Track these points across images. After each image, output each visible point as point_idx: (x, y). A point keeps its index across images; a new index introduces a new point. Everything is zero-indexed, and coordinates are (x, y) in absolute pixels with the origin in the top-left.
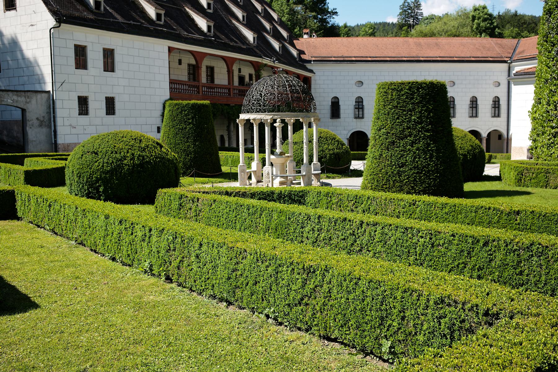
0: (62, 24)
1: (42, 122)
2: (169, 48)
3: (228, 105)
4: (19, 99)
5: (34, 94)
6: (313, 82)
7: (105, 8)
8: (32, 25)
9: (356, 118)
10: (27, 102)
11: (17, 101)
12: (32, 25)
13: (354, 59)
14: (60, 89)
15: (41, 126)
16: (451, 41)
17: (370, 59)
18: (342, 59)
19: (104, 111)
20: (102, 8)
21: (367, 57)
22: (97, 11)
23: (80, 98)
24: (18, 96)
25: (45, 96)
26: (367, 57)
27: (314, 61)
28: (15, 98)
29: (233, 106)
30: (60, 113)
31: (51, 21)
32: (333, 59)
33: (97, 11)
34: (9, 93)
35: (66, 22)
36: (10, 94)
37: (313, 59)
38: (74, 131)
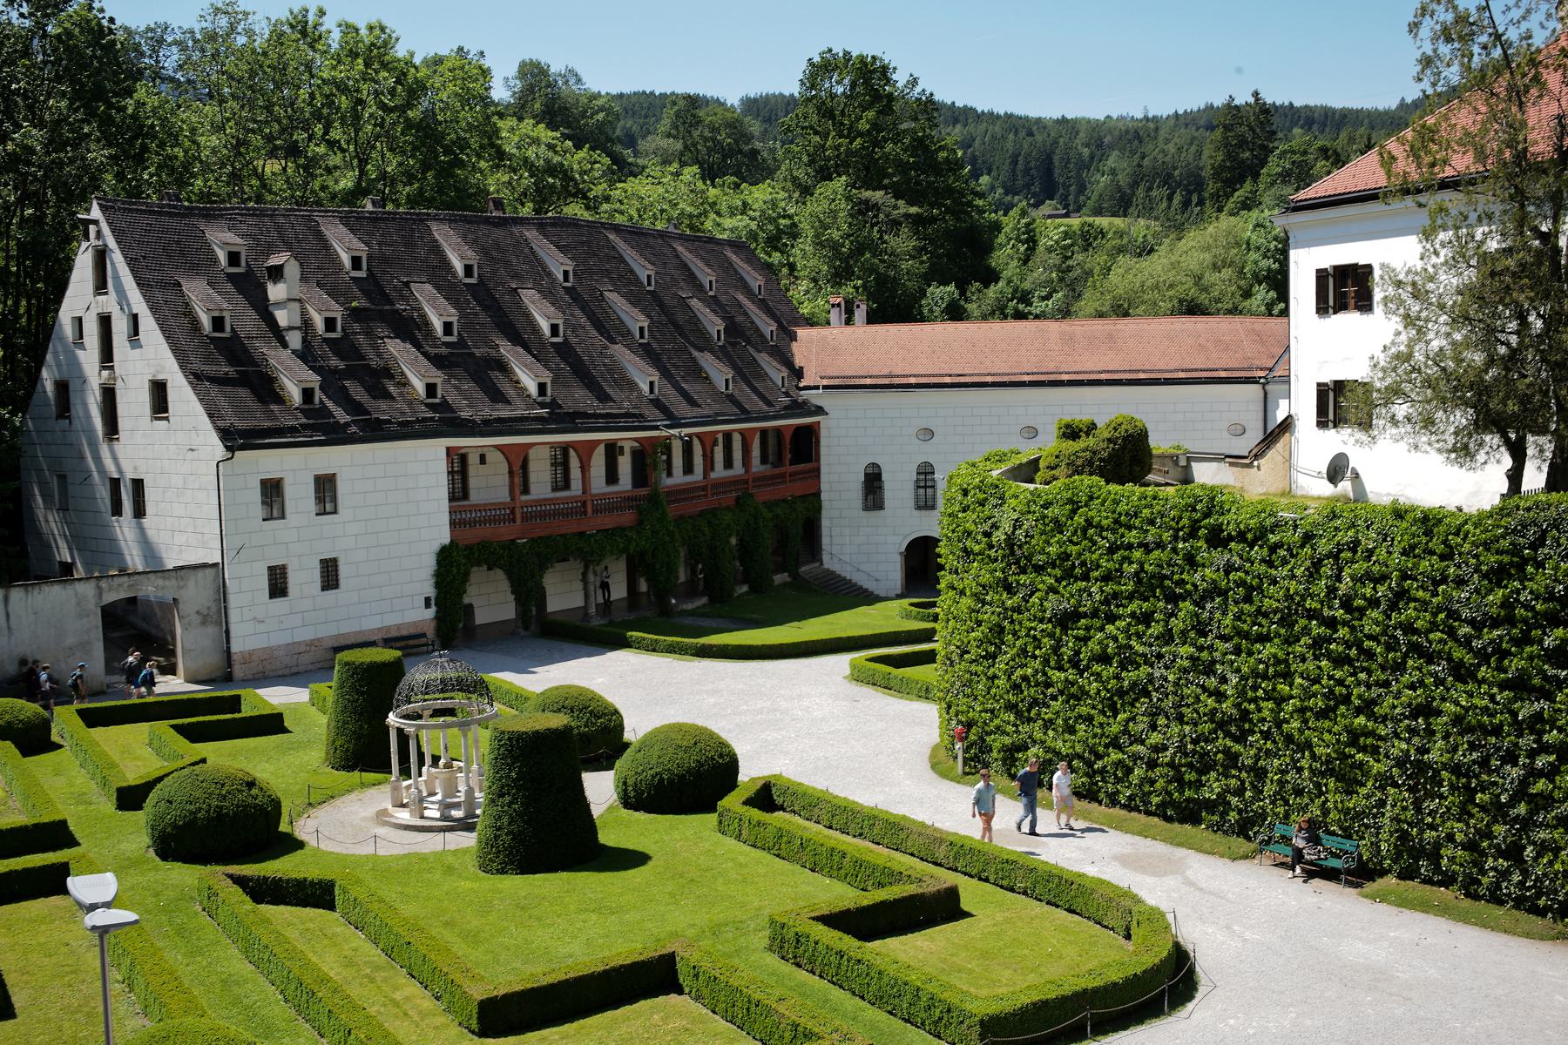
0: (238, 454)
1: (205, 616)
2: (448, 449)
3: (582, 534)
4: (167, 583)
5: (192, 572)
6: (823, 433)
7: (321, 401)
8: (192, 450)
9: (919, 508)
10: (180, 588)
11: (163, 588)
12: (192, 450)
13: (913, 380)
14: (236, 560)
15: (204, 623)
16: (1146, 327)
17: (948, 380)
18: (886, 381)
19: (318, 585)
20: (317, 400)
21: (942, 376)
22: (307, 407)
23: (272, 570)
24: (164, 578)
25: (210, 572)
26: (942, 376)
27: (825, 387)
28: (160, 582)
29: (591, 535)
30: (234, 601)
31: (217, 448)
32: (868, 381)
33: (307, 407)
34: (150, 575)
35: (243, 448)
36: (152, 576)
37: (825, 382)
38: (261, 628)
